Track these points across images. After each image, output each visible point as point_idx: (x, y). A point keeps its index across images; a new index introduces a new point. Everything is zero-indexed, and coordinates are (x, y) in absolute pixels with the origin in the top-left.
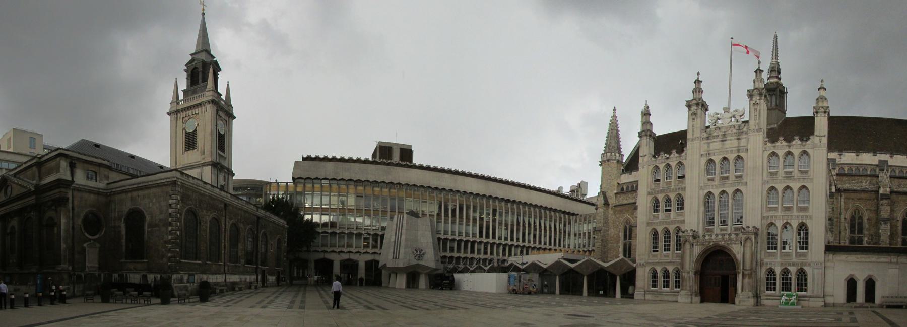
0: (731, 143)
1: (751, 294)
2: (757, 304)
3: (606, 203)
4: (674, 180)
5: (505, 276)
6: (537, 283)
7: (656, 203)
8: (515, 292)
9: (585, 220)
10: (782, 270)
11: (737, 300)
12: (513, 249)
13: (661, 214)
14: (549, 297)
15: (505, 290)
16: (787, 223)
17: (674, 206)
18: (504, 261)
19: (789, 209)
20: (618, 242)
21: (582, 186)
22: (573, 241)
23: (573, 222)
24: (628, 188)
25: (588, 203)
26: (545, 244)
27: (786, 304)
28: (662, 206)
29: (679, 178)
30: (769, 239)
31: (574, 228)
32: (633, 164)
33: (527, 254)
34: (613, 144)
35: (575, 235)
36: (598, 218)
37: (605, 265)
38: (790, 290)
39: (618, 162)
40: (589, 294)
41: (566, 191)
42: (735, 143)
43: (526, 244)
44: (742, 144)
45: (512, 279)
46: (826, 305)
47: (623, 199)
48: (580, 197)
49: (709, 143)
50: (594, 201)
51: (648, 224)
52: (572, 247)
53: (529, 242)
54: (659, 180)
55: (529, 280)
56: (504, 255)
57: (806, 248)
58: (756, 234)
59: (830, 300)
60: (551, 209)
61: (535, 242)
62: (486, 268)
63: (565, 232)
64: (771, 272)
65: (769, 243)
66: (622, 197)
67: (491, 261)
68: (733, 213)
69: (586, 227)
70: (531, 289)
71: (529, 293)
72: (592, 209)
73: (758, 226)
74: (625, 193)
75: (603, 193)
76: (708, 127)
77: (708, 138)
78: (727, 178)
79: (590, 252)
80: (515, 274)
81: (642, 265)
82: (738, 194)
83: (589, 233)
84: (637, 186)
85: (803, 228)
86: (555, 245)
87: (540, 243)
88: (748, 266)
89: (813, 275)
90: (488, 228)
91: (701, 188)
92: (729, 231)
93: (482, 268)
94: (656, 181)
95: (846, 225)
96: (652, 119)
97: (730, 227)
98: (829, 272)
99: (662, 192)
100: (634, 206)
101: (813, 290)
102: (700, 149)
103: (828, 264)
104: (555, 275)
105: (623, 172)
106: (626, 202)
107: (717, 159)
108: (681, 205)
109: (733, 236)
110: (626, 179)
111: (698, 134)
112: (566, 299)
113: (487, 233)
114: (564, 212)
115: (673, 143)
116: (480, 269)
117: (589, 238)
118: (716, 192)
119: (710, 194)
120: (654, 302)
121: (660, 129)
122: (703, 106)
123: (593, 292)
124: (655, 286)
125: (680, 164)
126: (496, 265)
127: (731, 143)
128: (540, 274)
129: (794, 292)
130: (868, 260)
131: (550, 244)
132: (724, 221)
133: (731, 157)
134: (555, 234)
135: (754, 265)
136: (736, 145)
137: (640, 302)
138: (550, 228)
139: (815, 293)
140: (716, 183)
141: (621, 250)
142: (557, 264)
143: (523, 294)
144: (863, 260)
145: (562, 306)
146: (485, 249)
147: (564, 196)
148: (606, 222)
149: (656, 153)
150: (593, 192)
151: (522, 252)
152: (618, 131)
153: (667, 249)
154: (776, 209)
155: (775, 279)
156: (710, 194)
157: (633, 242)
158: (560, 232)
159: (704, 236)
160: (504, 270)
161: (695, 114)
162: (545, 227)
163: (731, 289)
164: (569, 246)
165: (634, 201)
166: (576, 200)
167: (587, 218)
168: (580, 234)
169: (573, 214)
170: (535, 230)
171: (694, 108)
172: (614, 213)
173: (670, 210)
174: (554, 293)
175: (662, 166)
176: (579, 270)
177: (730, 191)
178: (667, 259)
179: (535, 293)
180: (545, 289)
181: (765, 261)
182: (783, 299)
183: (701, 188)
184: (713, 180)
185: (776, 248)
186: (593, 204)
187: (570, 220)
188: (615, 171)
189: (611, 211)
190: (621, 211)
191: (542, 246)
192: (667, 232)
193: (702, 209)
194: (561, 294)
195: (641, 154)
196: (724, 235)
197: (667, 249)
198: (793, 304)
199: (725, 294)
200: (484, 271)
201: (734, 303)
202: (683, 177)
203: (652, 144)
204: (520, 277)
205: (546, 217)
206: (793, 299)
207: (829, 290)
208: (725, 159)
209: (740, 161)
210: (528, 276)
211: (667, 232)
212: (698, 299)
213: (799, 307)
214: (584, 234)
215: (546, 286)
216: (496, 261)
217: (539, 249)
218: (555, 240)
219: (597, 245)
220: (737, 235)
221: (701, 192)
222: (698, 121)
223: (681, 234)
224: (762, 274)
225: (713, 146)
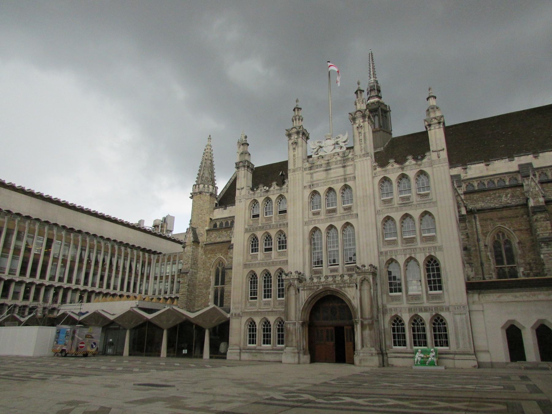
0: (337, 172)
1: (374, 350)
2: (384, 363)
3: (196, 241)
4: (274, 215)
5: (51, 331)
6: (98, 341)
7: (254, 241)
8: (64, 354)
9: (169, 260)
10: (412, 318)
11: (356, 359)
12: (70, 293)
13: (260, 254)
14: (114, 360)
15: (48, 352)
16: (411, 258)
17: (275, 244)
18: (54, 309)
19: (411, 240)
20: (208, 287)
21: (168, 221)
22: (152, 286)
23: (153, 262)
24: (221, 224)
25: (174, 241)
26: (115, 288)
27: (423, 363)
28: (261, 246)
29: (280, 212)
30: (390, 278)
31: (155, 270)
32: (228, 198)
33: (89, 301)
34: (206, 175)
35: (156, 278)
36: (184, 257)
37: (192, 315)
38: (425, 344)
39: (211, 194)
40: (169, 354)
41: (148, 225)
42: (341, 171)
43: (89, 288)
44: (348, 172)
45: (62, 336)
46: (480, 365)
47: (217, 237)
48: (165, 234)
49: (312, 174)
50: (181, 239)
51: (245, 266)
52: (150, 293)
53: (93, 285)
54: (258, 216)
55: (87, 336)
56: (55, 301)
57: (440, 288)
58: (374, 274)
59: (484, 358)
60: (127, 245)
61: (101, 286)
62: (22, 320)
63: (142, 274)
64: (397, 321)
65: (391, 284)
66: (214, 234)
67: (32, 309)
68: (344, 250)
69: (169, 269)
70: (89, 349)
71: (86, 355)
72: (178, 248)
73: (376, 264)
74: (218, 230)
75: (193, 230)
76: (311, 157)
77: (311, 168)
78: (334, 211)
79: (172, 299)
80: (68, 328)
81: (239, 316)
82: (349, 228)
83: (173, 276)
84: (233, 222)
85: (433, 266)
86: (128, 290)
87: (108, 286)
88: (367, 314)
89: (454, 321)
90: (35, 264)
91: (306, 223)
92: (341, 272)
93: (16, 319)
94: (254, 216)
95: (488, 255)
96: (249, 149)
97: (341, 268)
98: (477, 318)
99: (261, 228)
100: (228, 245)
101: (457, 344)
102: (303, 181)
103: (474, 307)
104: (125, 329)
105: (217, 206)
106: (219, 240)
107: (322, 190)
108: (283, 245)
109: (346, 278)
110: (220, 214)
111: (299, 164)
112: (139, 360)
113: (34, 270)
114: (144, 250)
115: (271, 176)
116: (13, 321)
117: (173, 282)
118: (323, 227)
119: (316, 229)
120: (250, 363)
121: (258, 162)
122: (303, 134)
123: (175, 350)
124: (252, 342)
125: (281, 197)
126: (39, 315)
127: (337, 172)
128: (103, 328)
129: (431, 347)
130: (535, 298)
131: (122, 289)
132: (334, 261)
133: (338, 187)
134: (130, 276)
135: (375, 313)
136: (342, 174)
137: (233, 364)
138: (124, 268)
139: (462, 348)
140: (323, 216)
141: (211, 297)
142: (130, 314)
143: (76, 356)
144: (525, 298)
145: (130, 372)
146: (27, 292)
147: (145, 231)
148: (195, 262)
149: (255, 186)
150: (180, 228)
151: (81, 298)
152: (212, 161)
153: (267, 294)
154: (394, 242)
155: (403, 330)
156: (316, 229)
157: (226, 288)
158: (136, 274)
159: (311, 279)
160: (52, 322)
161: (296, 143)
162: (117, 267)
163: (348, 345)
164: (146, 293)
165: (228, 239)
166: (160, 236)
167: (172, 258)
168: (161, 277)
169: (155, 253)
170: (103, 270)
171: (294, 137)
172: (205, 252)
173: (270, 249)
174: (121, 354)
175: (261, 200)
176: (157, 322)
177: (339, 225)
178: (267, 308)
179: (94, 355)
180: (109, 349)
181: (389, 306)
182: (418, 356)
183: (306, 223)
184: (318, 213)
185: (400, 291)
186: (179, 242)
187: (150, 260)
188: (207, 206)
189: (200, 250)
190: (213, 251)
191: (111, 291)
192: (267, 275)
193: (307, 247)
194: (130, 355)
195: (238, 186)
196: (334, 277)
197: (267, 294)
198: (432, 364)
199: (342, 353)
200: (20, 324)
201: (353, 363)
202: (285, 212)
203: (250, 176)
204: (74, 332)
205: (119, 255)
206: (432, 357)
207: (481, 343)
208: (330, 189)
209: (347, 190)
210: (86, 331)
211: (267, 275)
212: (306, 358)
213: (441, 368)
214: (167, 277)
215: (111, 344)
216: (40, 309)
217: (106, 295)
218: (129, 283)
219: (182, 290)
220: (350, 276)
221: (306, 227)
222: (299, 151)
223: (284, 277)
224: (386, 323)
225: (316, 176)
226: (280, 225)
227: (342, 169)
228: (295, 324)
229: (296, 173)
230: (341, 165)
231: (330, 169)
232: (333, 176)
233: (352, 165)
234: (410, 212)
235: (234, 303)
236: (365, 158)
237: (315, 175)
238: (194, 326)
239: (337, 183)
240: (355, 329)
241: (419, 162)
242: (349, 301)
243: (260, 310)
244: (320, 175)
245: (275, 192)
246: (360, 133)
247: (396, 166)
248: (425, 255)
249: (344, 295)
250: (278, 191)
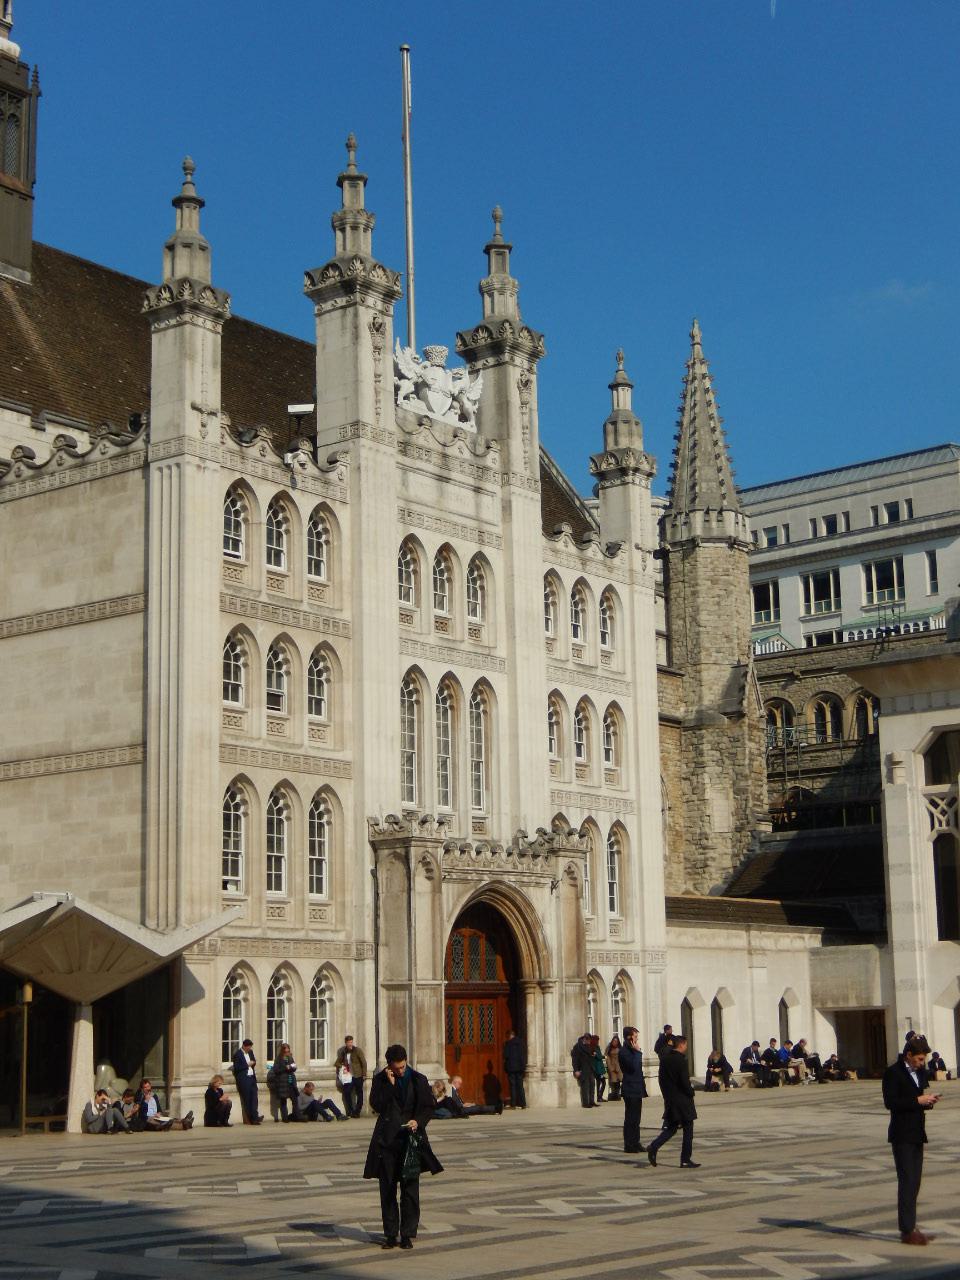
118: (434, 673)
136: (470, 510)
226: (326, 622)
227: (471, 494)
228: (434, 988)
229: (383, 448)
230: (471, 481)
231: (447, 480)
232: (453, 505)
233: (493, 494)
234: (593, 695)
235: (192, 901)
236: (531, 494)
237: (411, 476)
238: (28, 993)
239: (464, 538)
240: (530, 1009)
241: (608, 560)
242: (531, 929)
243: (271, 934)
244: (422, 487)
245: (310, 484)
246: (524, 404)
247: (572, 549)
248: (611, 818)
249: (524, 908)
250: (319, 487)
